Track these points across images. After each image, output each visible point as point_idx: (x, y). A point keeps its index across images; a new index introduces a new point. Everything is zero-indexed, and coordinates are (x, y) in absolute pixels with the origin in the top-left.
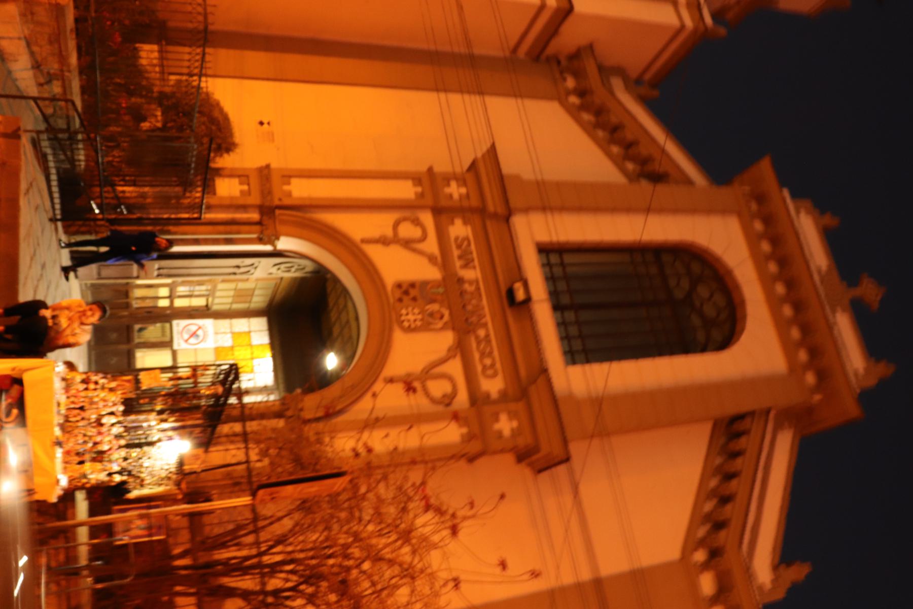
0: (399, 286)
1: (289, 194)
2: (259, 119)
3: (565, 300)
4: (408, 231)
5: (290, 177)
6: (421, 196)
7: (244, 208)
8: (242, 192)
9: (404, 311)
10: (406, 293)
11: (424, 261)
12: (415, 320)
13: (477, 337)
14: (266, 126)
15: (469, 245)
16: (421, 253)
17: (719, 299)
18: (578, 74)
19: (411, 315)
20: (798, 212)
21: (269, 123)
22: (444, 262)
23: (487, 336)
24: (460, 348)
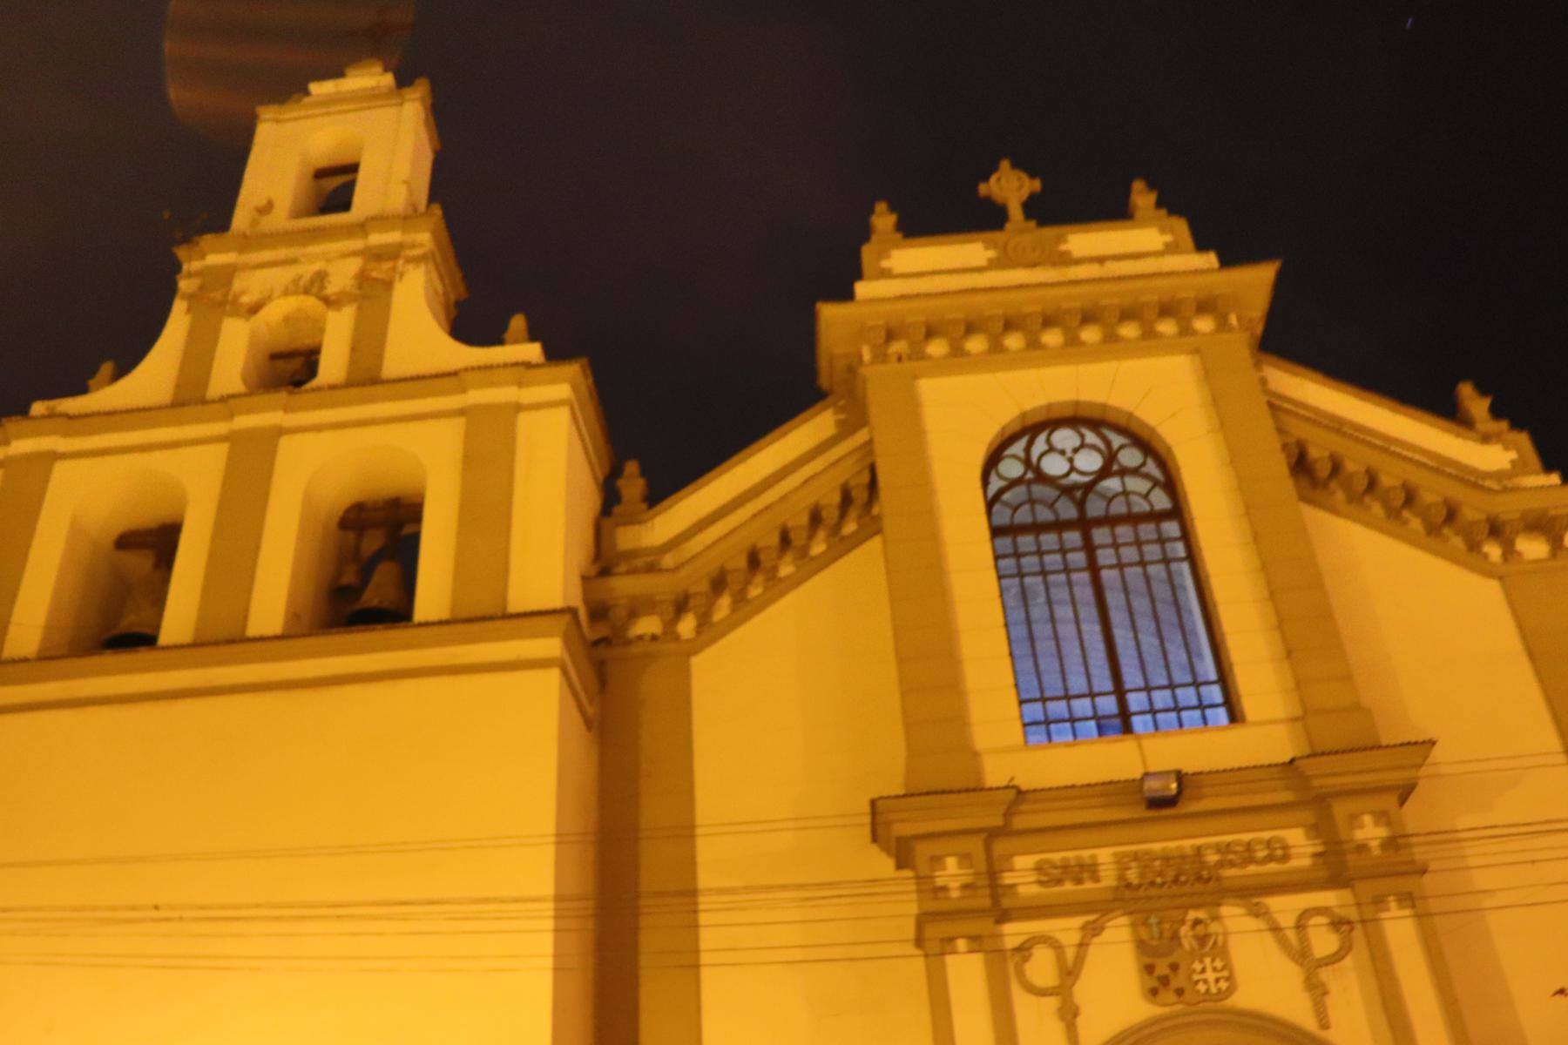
0: (1154, 992)
4: (1042, 967)
6: (975, 940)
9: (1202, 987)
10: (1165, 981)
12: (1215, 970)
13: (1221, 864)
19: (1207, 975)
20: (886, 274)
22: (1098, 910)
23: (1218, 848)
24: (1251, 894)
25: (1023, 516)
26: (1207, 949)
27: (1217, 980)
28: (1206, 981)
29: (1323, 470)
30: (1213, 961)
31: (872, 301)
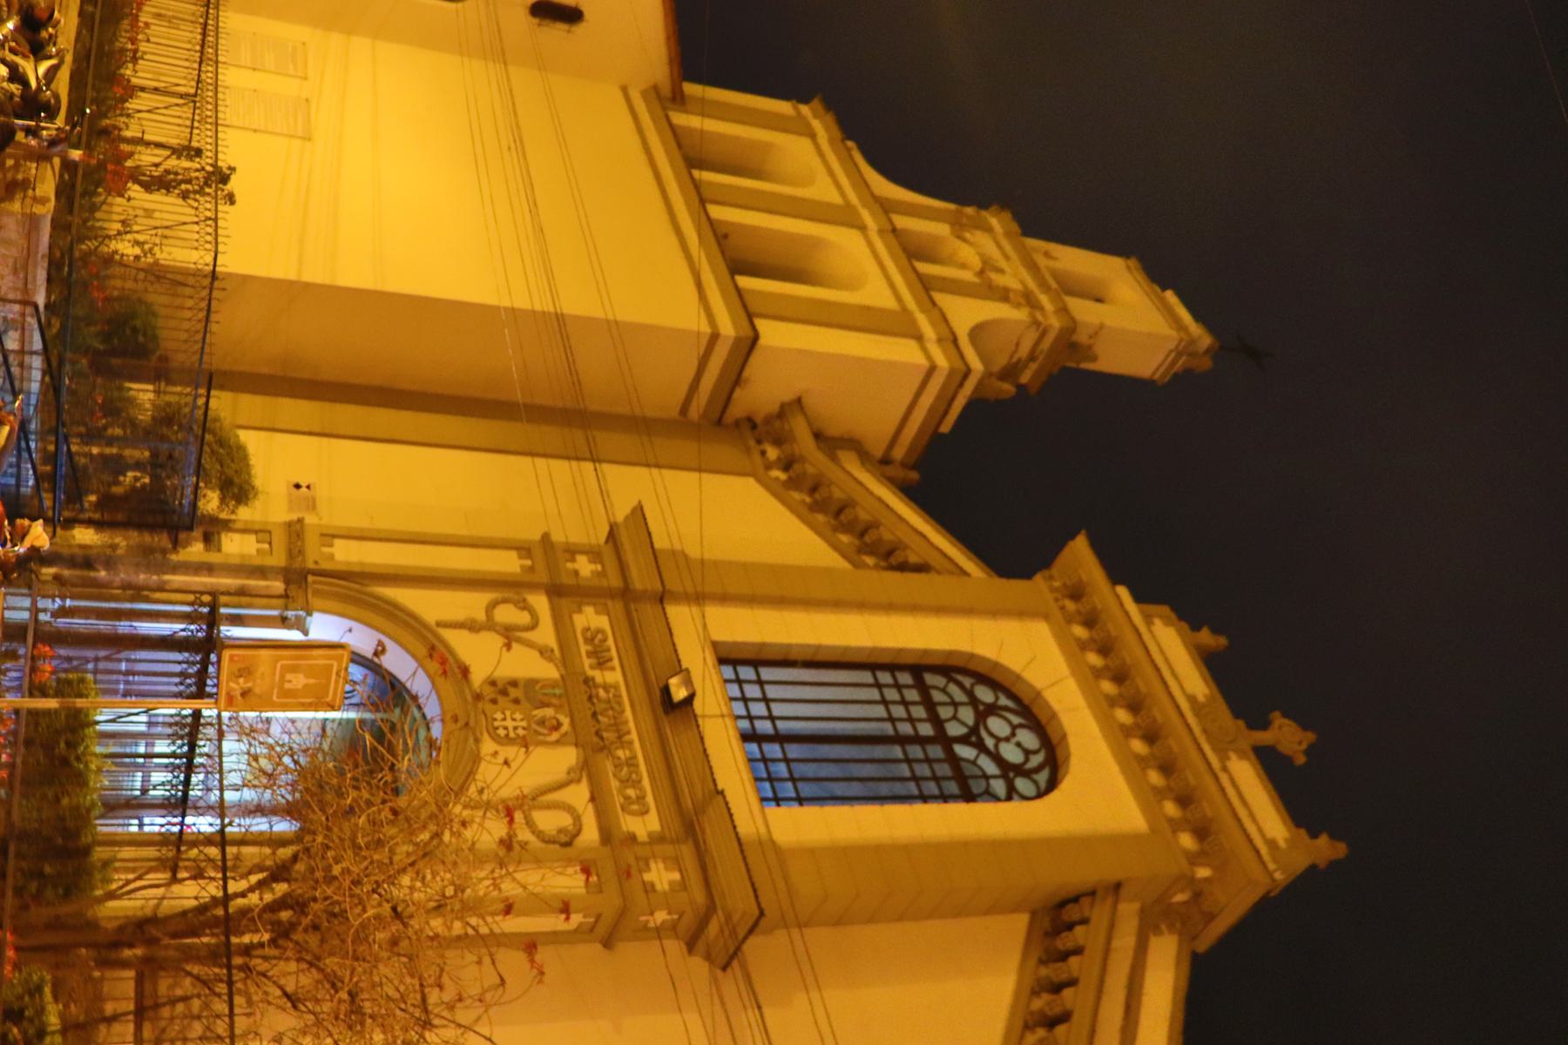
0: (493, 683)
1: (331, 557)
2: (296, 480)
3: (764, 727)
5: (334, 536)
7: (261, 572)
8: (258, 551)
9: (499, 716)
10: (504, 693)
11: (536, 654)
12: (515, 728)
14: (304, 490)
15: (605, 640)
16: (530, 644)
17: (1028, 739)
18: (778, 442)
19: (511, 720)
20: (1148, 620)
21: (308, 487)
22: (565, 654)
23: (631, 763)
24: (586, 769)
25: (938, 696)
26: (535, 726)
27: (506, 728)
28: (504, 719)
29: (1065, 941)
30: (524, 728)
31: (1118, 596)
